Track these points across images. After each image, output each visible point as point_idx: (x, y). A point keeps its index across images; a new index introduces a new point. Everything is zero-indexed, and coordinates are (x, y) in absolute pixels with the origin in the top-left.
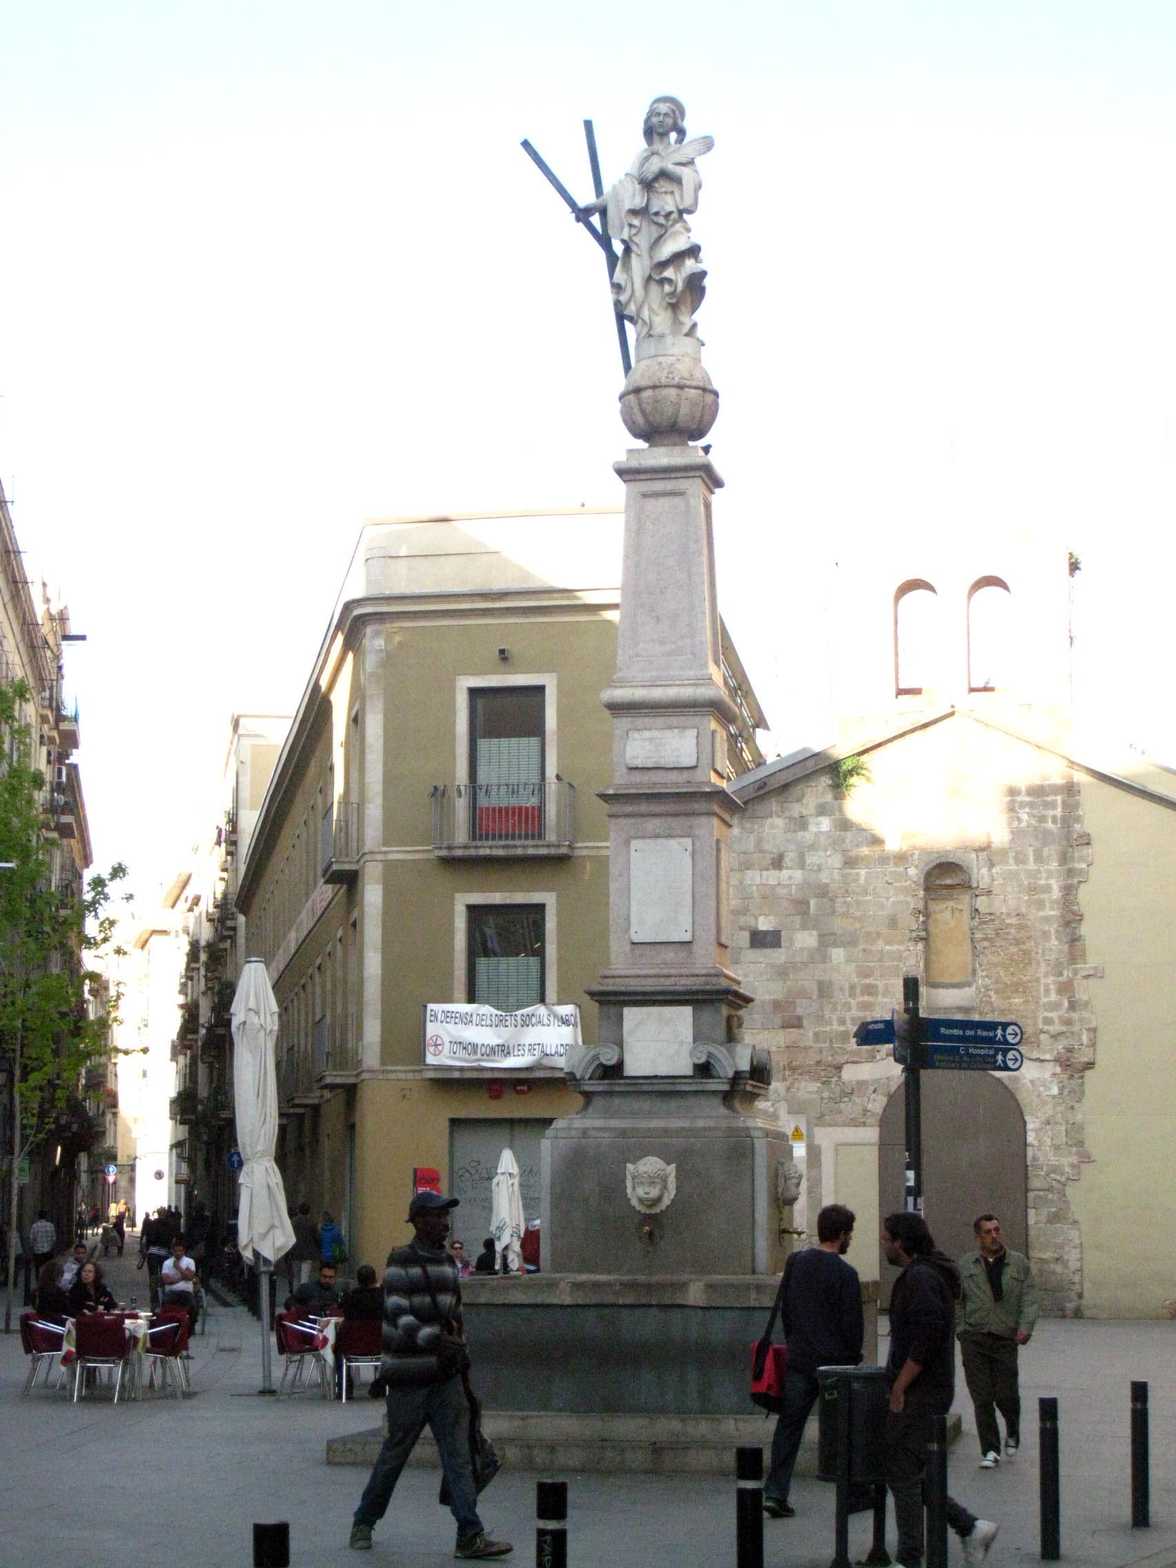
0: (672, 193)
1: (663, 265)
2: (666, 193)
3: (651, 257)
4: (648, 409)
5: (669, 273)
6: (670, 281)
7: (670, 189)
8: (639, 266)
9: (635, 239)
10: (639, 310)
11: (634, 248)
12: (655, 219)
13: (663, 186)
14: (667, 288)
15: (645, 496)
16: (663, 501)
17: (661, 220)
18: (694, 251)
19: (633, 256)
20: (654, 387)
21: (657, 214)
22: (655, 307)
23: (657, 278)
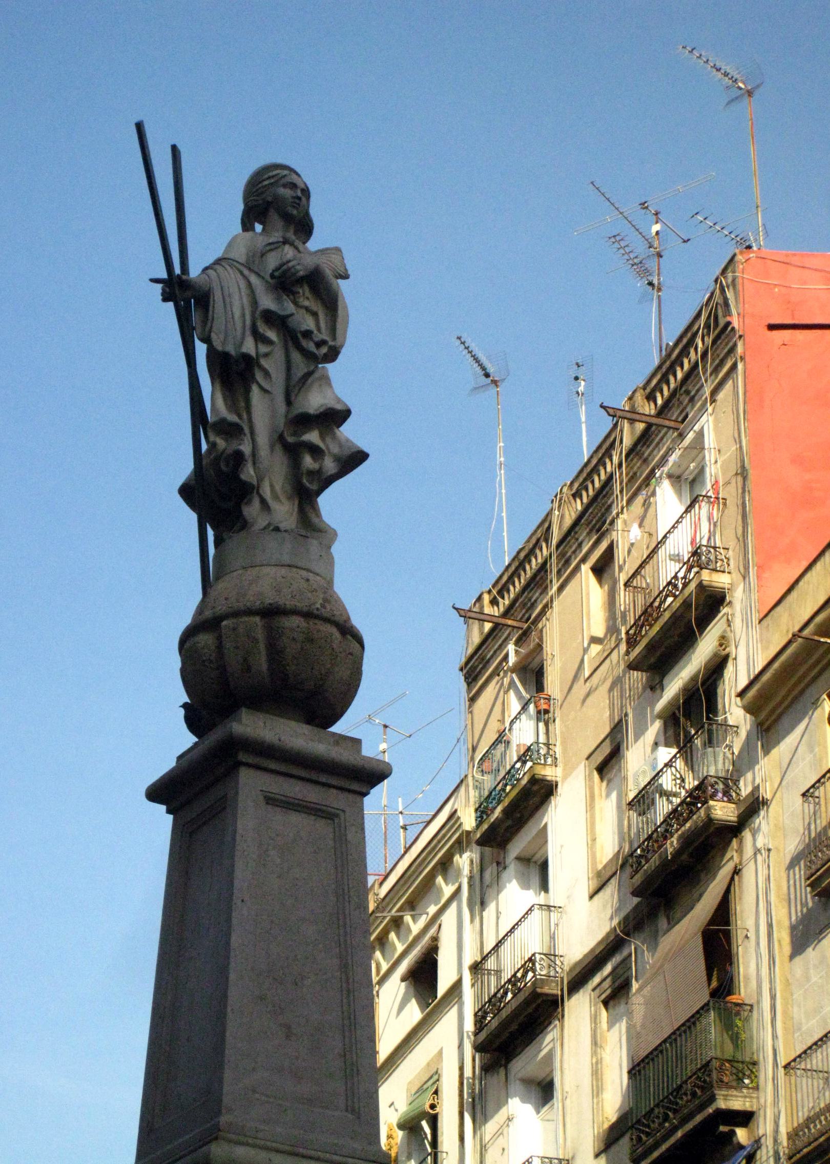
0: (315, 314)
1: (304, 421)
2: (307, 309)
3: (289, 403)
4: (292, 649)
5: (313, 437)
6: (316, 452)
7: (315, 308)
8: (264, 412)
9: (263, 362)
10: (260, 479)
11: (259, 376)
12: (304, 343)
13: (307, 299)
14: (308, 461)
15: (271, 800)
16: (295, 818)
17: (311, 347)
18: (336, 417)
19: (255, 388)
20: (308, 615)
21: (307, 334)
22: (278, 488)
23: (291, 439)
